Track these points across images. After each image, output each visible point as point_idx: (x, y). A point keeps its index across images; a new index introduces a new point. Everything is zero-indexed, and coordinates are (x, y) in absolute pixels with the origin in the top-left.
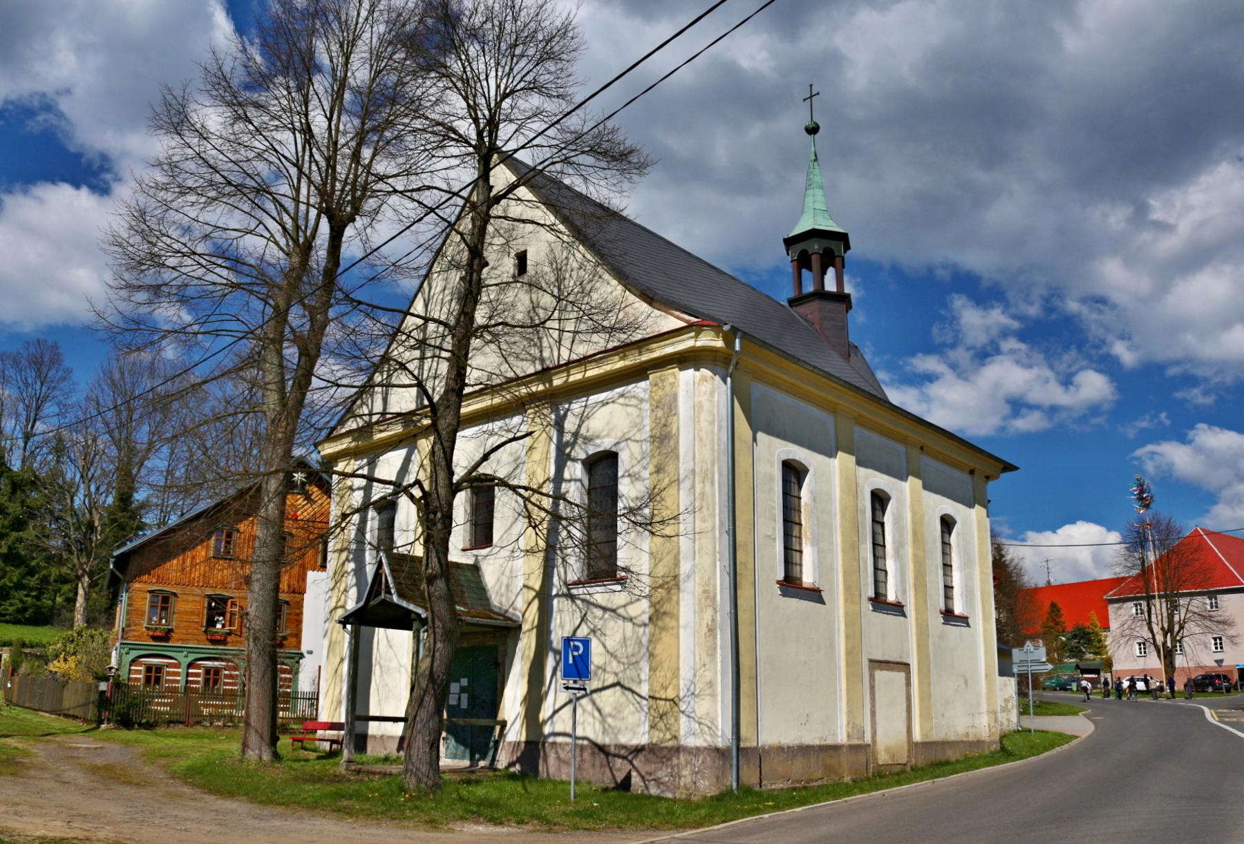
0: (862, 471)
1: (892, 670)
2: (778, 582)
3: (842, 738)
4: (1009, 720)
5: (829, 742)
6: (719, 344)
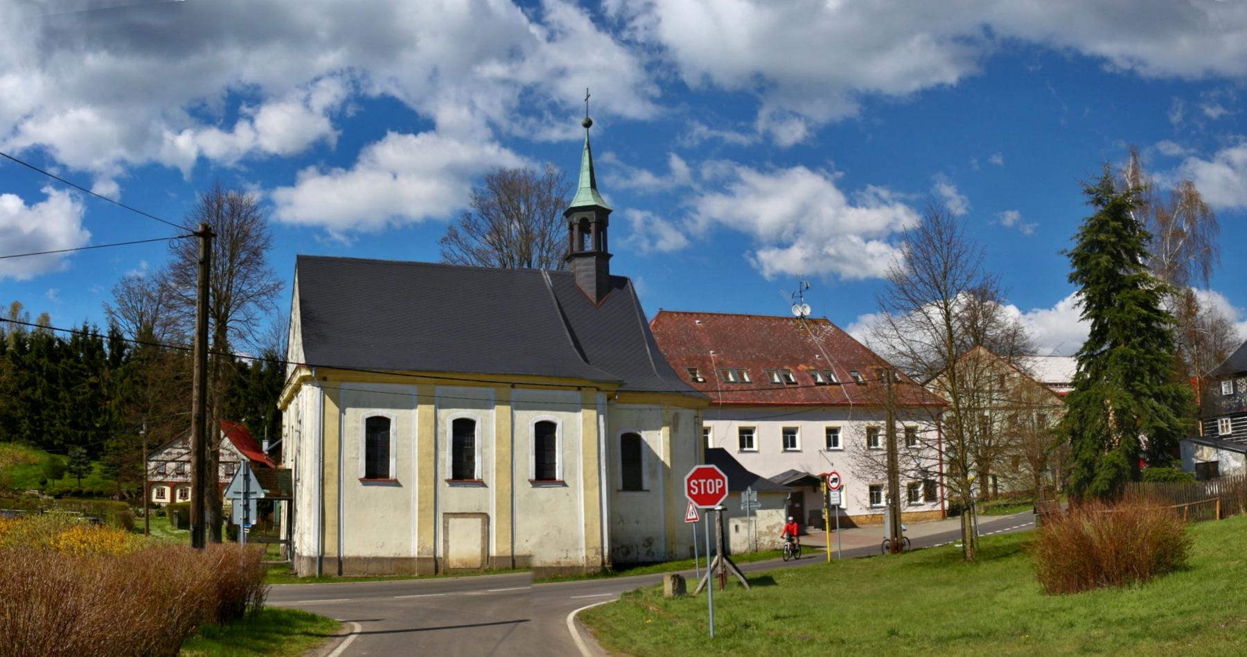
0: (443, 413)
2: (361, 480)
3: (414, 552)
5: (402, 555)
6: (308, 373)
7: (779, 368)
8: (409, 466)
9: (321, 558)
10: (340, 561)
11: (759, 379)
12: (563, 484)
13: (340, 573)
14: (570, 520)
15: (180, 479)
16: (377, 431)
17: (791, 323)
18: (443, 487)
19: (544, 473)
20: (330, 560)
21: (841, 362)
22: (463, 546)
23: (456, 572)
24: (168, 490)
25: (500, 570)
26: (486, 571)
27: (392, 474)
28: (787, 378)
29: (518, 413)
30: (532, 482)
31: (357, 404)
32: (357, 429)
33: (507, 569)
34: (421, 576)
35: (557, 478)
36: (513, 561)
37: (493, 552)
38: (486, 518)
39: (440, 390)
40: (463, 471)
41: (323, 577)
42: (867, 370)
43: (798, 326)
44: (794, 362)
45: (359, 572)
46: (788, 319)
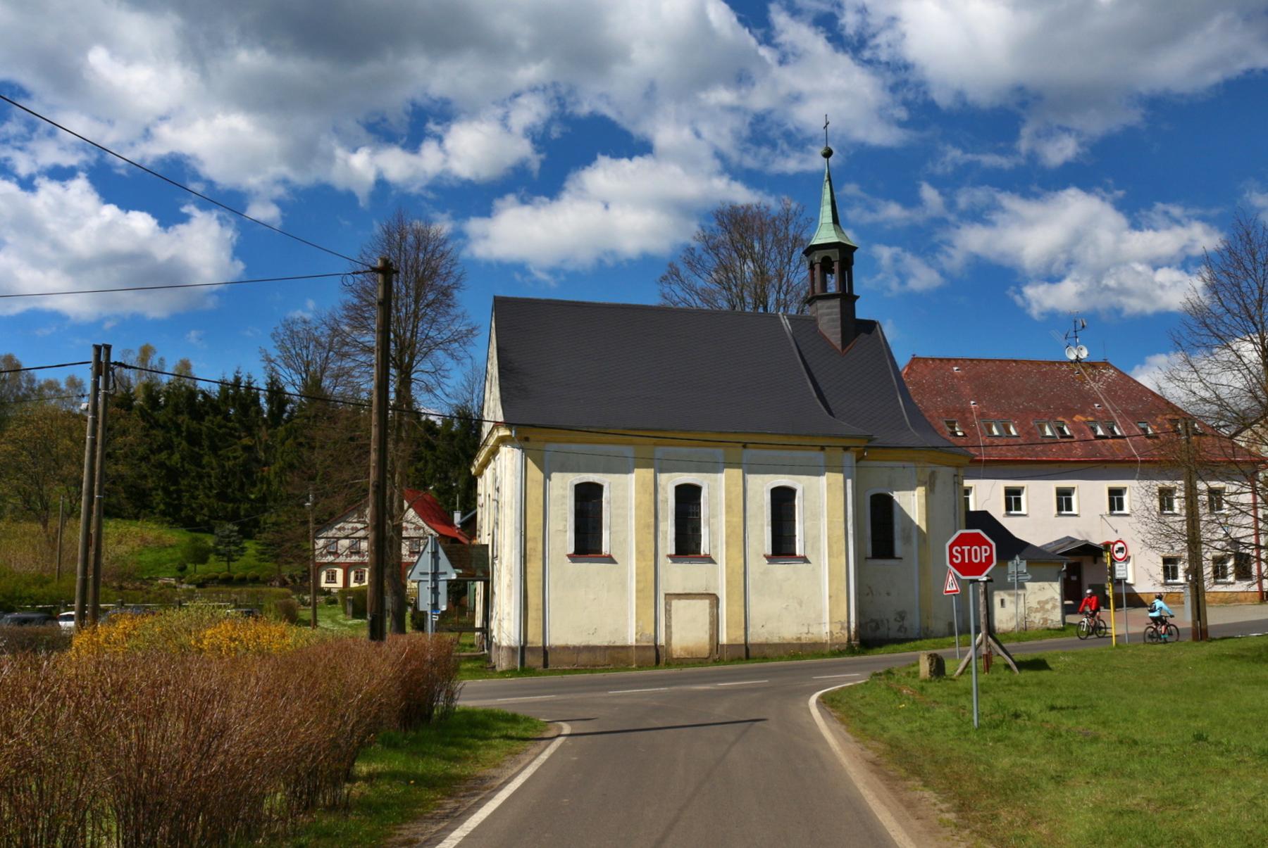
2: (569, 556)
3: (631, 640)
4: (1046, 620)
6: (508, 433)
7: (1051, 419)
9: (523, 648)
10: (545, 651)
11: (1028, 433)
12: (805, 560)
13: (546, 665)
14: (812, 598)
15: (355, 558)
16: (588, 498)
17: (1065, 368)
18: (665, 562)
19: (782, 547)
20: (533, 650)
21: (1126, 411)
22: (688, 631)
23: (681, 662)
24: (340, 573)
25: (732, 661)
26: (715, 662)
27: (605, 549)
28: (1062, 431)
29: (750, 477)
31: (564, 469)
32: (564, 497)
33: (739, 660)
34: (640, 667)
35: (798, 553)
36: (747, 650)
37: (724, 639)
38: (714, 599)
39: (660, 452)
40: (687, 545)
41: (525, 670)
42: (1159, 420)
43: (1072, 371)
44: (1069, 413)
45: (568, 664)
46: (1061, 363)
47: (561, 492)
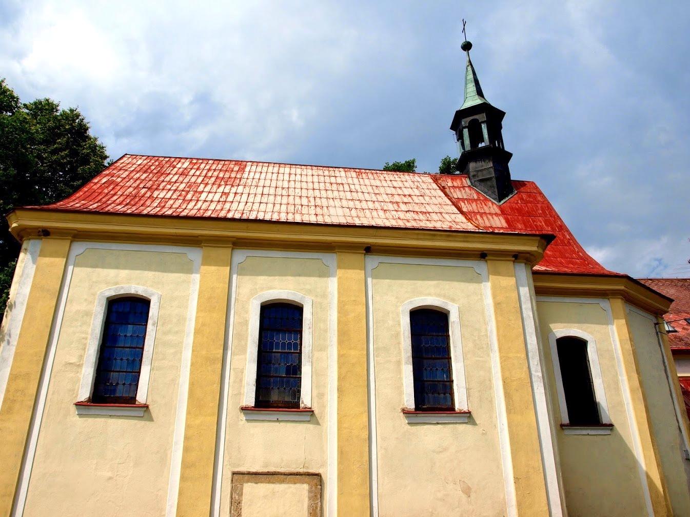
1: (282, 482)
8: (174, 382)
12: (468, 416)
19: (433, 393)
30: (406, 412)
32: (88, 314)
35: (458, 406)
47: (83, 307)
